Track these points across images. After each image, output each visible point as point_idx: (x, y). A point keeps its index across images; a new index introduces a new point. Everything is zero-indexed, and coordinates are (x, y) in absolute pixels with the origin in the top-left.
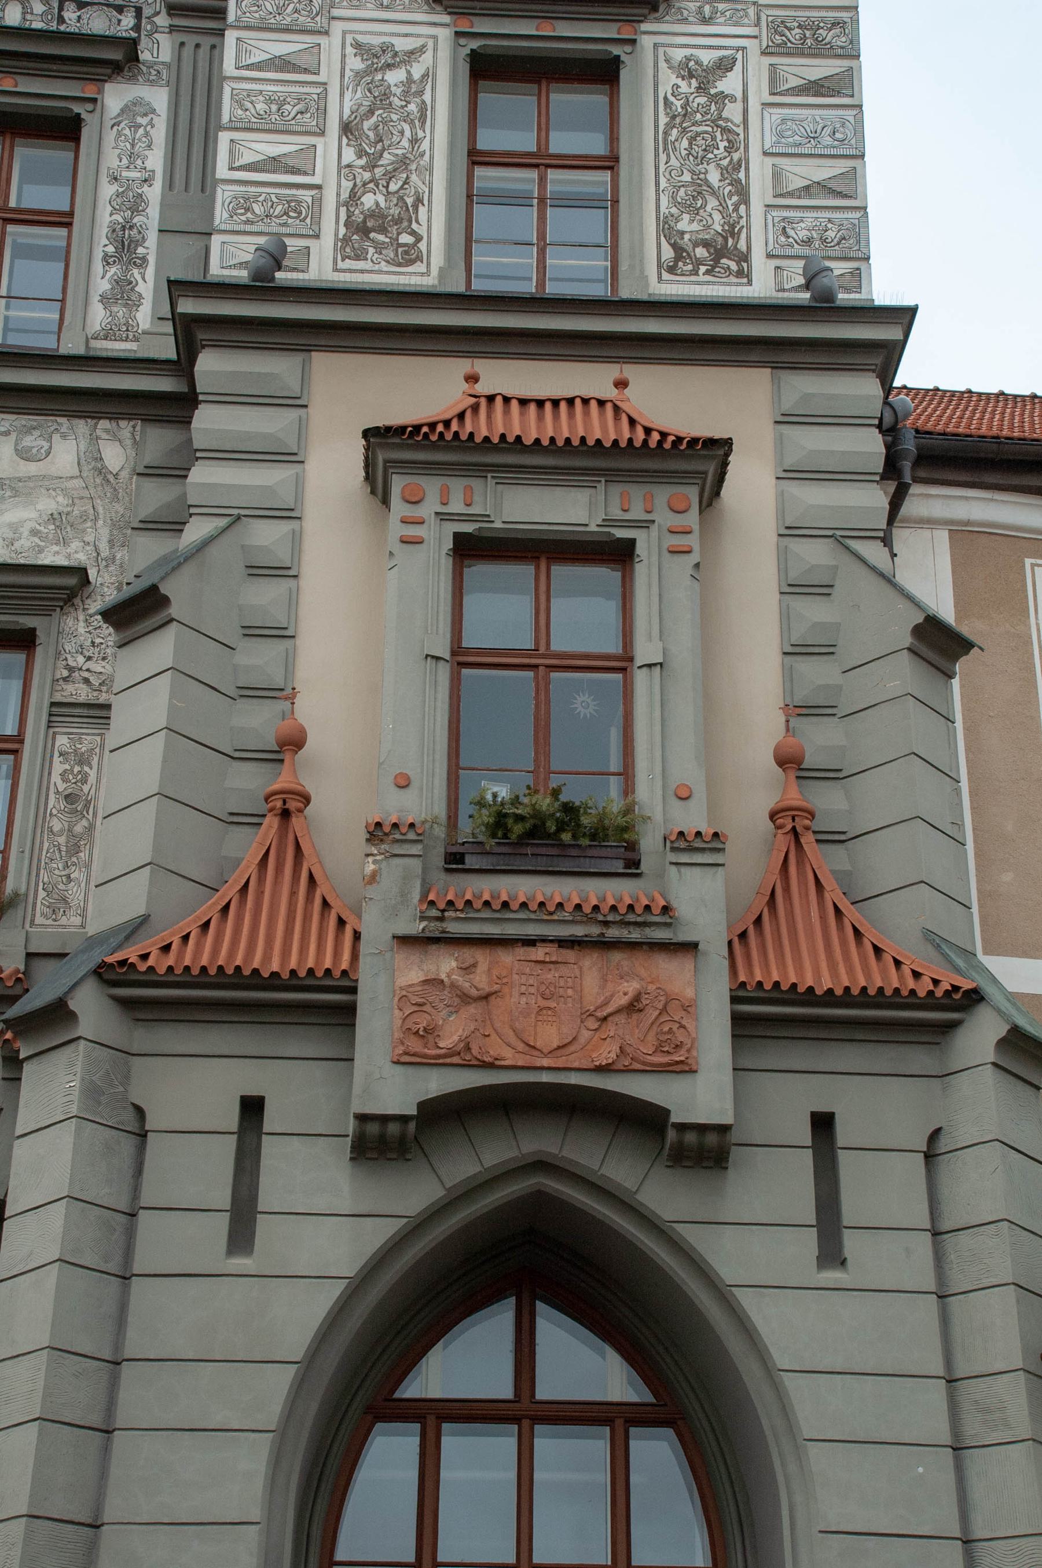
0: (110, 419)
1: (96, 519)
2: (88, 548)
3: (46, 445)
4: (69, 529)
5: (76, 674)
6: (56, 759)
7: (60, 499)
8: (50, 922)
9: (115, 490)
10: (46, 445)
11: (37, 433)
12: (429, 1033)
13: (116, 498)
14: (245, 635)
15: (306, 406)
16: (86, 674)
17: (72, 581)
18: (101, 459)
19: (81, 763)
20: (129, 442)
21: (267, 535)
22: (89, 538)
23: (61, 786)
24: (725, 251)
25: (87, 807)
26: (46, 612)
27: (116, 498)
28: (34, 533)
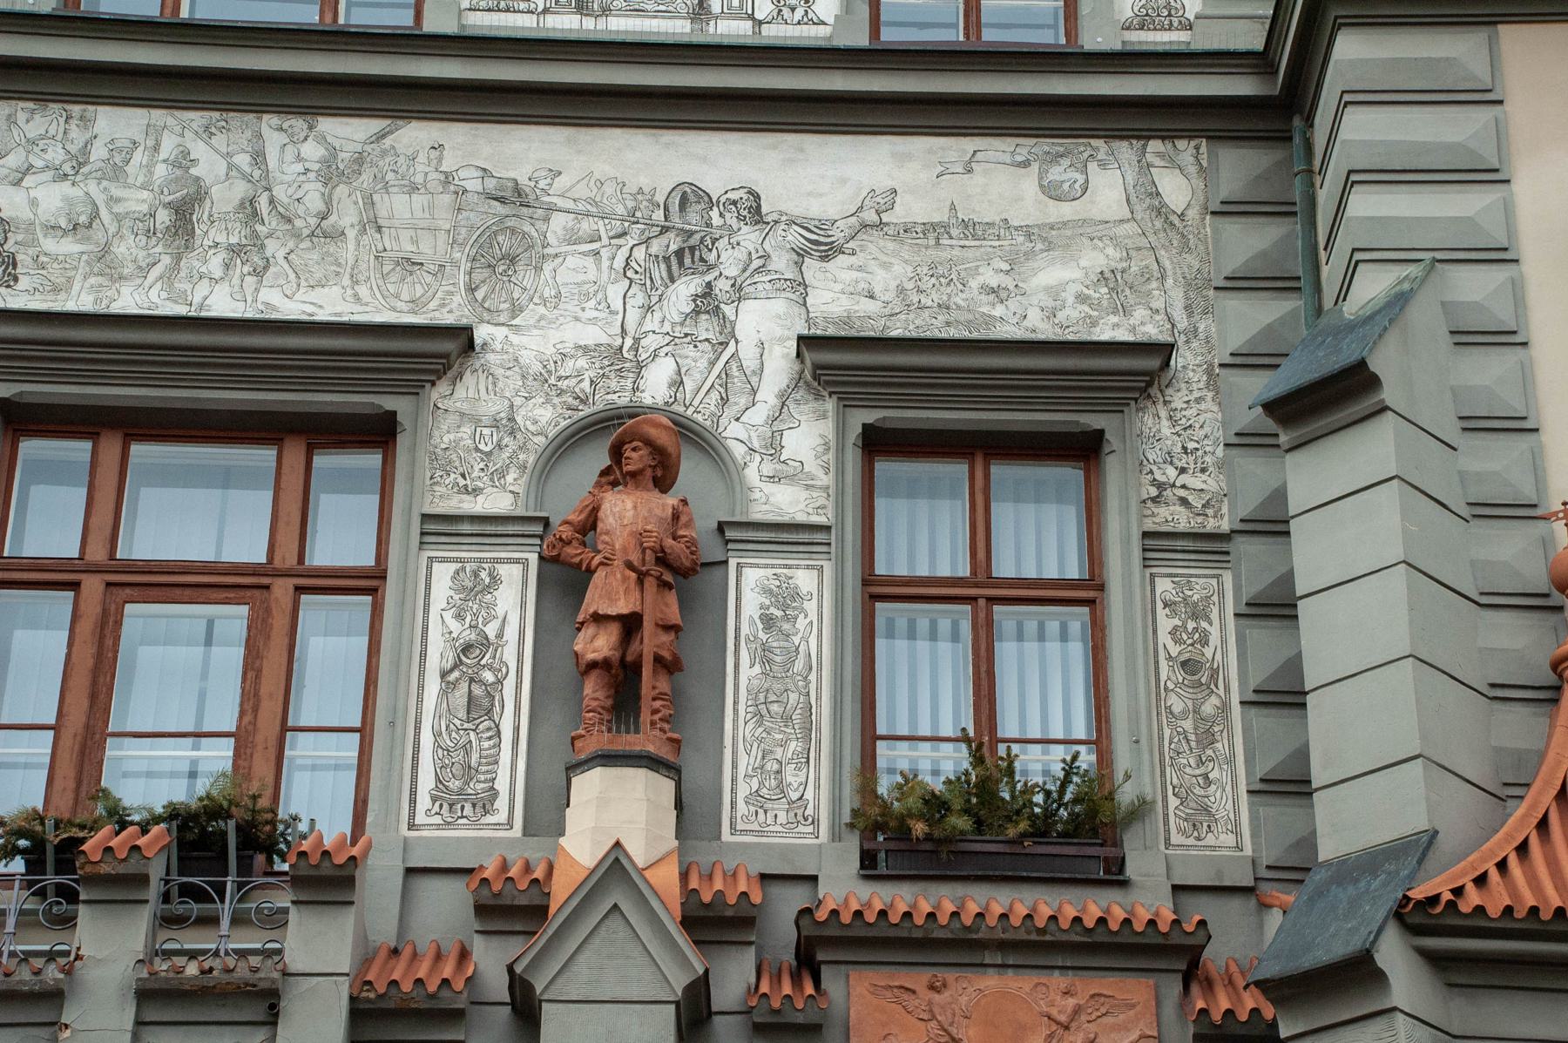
0: (1163, 138)
1: (1163, 278)
2: (1158, 318)
3: (1081, 178)
4: (1128, 292)
5: (1168, 493)
6: (1161, 612)
7: (1110, 251)
8: (1191, 841)
9: (1183, 236)
10: (1081, 178)
11: (1066, 162)
13: (1185, 247)
14: (1464, 429)
15: (1501, 102)
16: (1182, 493)
17: (1153, 363)
18: (1158, 194)
19: (1194, 617)
20: (1193, 169)
21: (1473, 287)
22: (1158, 304)
23: (1174, 650)
25: (1214, 674)
26: (1117, 407)
27: (1185, 247)
28: (1082, 299)
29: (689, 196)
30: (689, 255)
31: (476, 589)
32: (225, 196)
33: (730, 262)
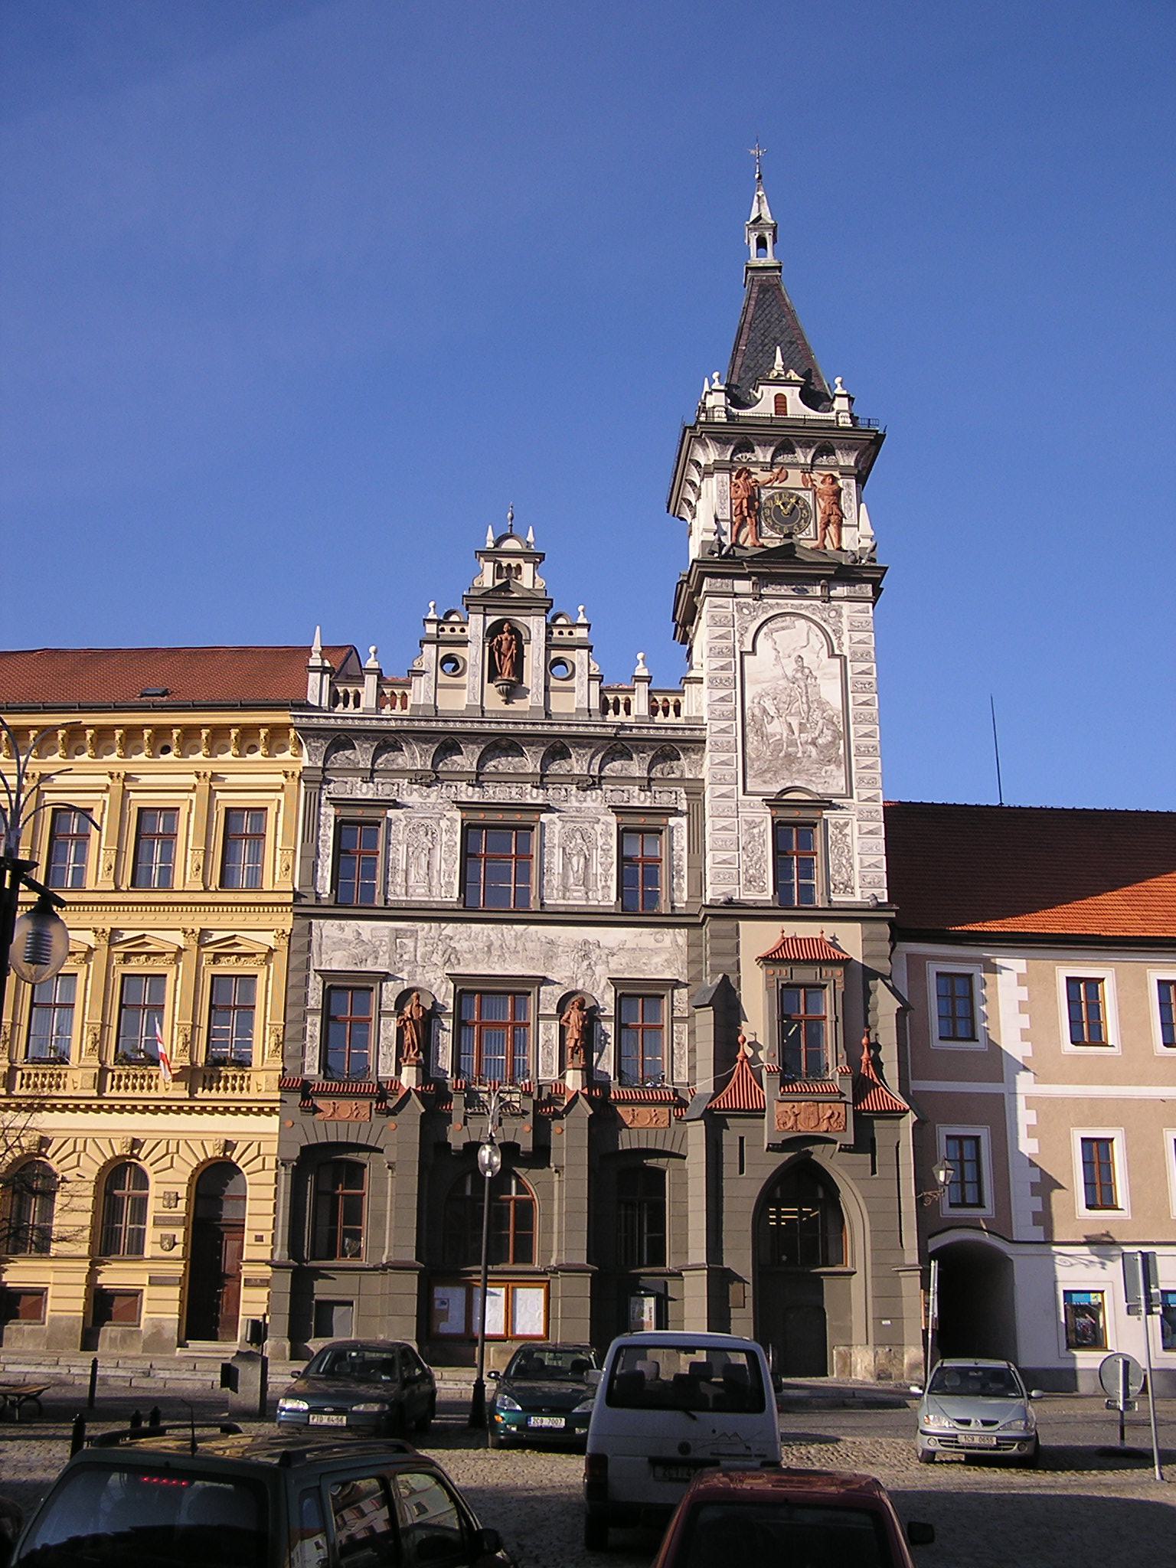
12: (785, 1123)
24: (847, 887)
29: (586, 942)
30: (586, 956)
31: (548, 1029)
32: (497, 944)
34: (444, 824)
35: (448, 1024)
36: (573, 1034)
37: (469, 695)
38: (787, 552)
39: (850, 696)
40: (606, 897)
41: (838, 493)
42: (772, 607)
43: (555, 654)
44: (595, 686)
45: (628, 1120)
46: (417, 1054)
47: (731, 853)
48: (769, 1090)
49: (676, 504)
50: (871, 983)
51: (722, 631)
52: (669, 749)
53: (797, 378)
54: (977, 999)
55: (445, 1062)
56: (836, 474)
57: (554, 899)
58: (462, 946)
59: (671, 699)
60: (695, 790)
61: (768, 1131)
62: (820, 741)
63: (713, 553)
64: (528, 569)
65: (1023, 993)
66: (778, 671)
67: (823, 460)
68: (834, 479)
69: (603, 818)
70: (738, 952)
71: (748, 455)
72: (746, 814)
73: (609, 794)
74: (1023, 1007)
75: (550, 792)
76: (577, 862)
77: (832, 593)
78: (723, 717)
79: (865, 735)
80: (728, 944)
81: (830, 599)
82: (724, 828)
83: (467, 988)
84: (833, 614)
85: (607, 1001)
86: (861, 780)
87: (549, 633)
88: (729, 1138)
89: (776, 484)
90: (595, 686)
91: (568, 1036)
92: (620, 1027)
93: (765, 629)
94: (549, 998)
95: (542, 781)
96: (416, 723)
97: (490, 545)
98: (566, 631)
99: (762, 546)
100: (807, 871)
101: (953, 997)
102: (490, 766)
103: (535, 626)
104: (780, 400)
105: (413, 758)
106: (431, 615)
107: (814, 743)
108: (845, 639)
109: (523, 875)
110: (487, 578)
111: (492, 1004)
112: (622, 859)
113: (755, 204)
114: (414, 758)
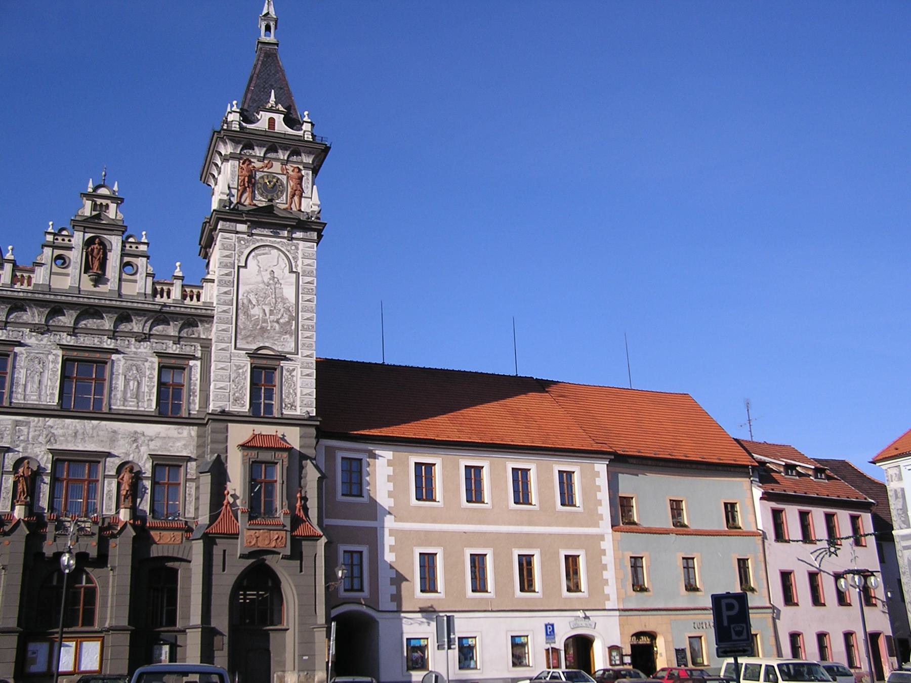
24: (293, 406)
29: (136, 432)
30: (135, 441)
31: (110, 484)
32: (81, 431)
33: (140, 441)
34: (51, 357)
35: (47, 479)
36: (125, 487)
37: (71, 280)
38: (269, 210)
39: (300, 296)
40: (150, 405)
41: (301, 178)
42: (258, 241)
43: (126, 259)
44: (150, 280)
45: (157, 539)
46: (26, 498)
47: (225, 383)
48: (242, 522)
49: (206, 176)
50: (304, 462)
51: (228, 253)
52: (194, 319)
53: (282, 109)
54: (364, 473)
55: (44, 503)
56: (301, 167)
57: (117, 406)
58: (58, 432)
59: (195, 291)
60: (206, 345)
61: (241, 546)
62: (281, 321)
63: (225, 207)
64: (113, 207)
65: (390, 471)
66: (259, 279)
67: (294, 158)
68: (300, 170)
69: (150, 359)
70: (227, 441)
71: (251, 151)
72: (235, 361)
73: (154, 345)
74: (390, 479)
75: (119, 342)
76: (133, 385)
77: (294, 236)
78: (225, 303)
79: (308, 319)
80: (221, 437)
81: (292, 239)
82: (222, 369)
83: (61, 458)
84: (293, 248)
85: (147, 468)
86: (304, 344)
87: (123, 246)
88: (217, 551)
89: (265, 170)
90: (150, 280)
91: (123, 488)
92: (154, 483)
93: (253, 254)
94: (112, 465)
95: (114, 335)
96: (36, 295)
97: (90, 190)
98: (134, 246)
99: (255, 205)
100: (269, 396)
101: (351, 471)
102: (82, 324)
103: (115, 241)
104: (272, 122)
105: (33, 316)
106: (50, 230)
107: (277, 322)
108: (300, 262)
109: (99, 390)
110: (87, 210)
111: (77, 468)
112: (161, 384)
113: (266, 5)
114: (34, 316)
